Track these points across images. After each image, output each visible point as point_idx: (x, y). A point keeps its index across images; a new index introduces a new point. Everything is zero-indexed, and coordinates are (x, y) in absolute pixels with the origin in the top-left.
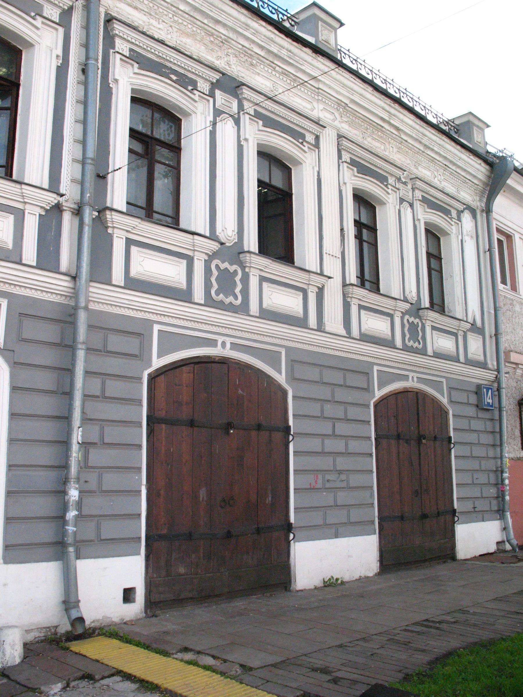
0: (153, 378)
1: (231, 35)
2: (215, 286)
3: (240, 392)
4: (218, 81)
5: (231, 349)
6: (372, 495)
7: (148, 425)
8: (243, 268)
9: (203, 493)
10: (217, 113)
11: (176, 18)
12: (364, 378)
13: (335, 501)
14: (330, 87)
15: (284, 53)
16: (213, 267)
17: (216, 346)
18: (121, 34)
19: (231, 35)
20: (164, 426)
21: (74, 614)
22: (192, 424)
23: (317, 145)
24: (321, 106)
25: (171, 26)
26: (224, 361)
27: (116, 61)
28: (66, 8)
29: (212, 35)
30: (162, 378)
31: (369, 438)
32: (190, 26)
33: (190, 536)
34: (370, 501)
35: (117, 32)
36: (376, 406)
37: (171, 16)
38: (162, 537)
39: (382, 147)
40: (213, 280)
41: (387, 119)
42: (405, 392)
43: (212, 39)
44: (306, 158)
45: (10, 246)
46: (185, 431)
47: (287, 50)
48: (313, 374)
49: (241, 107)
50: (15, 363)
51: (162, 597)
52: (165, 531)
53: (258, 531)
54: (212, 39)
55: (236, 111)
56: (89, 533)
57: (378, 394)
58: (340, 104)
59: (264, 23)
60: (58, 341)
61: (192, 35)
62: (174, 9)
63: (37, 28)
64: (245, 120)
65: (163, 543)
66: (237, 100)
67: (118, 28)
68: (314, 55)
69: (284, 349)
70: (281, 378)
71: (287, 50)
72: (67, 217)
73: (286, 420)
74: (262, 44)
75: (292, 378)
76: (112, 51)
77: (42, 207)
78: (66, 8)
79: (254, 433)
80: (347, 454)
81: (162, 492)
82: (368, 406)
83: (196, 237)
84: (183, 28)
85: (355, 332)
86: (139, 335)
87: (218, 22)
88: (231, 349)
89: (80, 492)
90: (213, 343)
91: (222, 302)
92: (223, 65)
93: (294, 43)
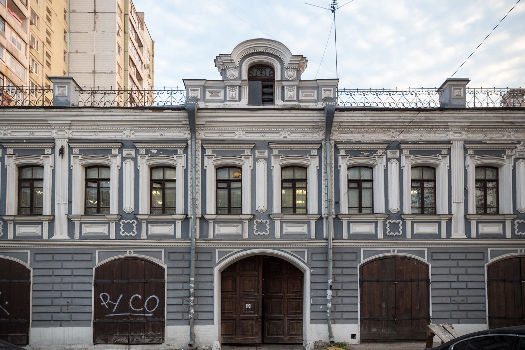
0: (362, 267)
1: (392, 124)
2: (389, 230)
3: (401, 268)
4: (387, 147)
5: (397, 252)
6: (485, 307)
7: (360, 282)
8: (402, 219)
9: (384, 305)
10: (388, 160)
11: (365, 129)
12: (481, 255)
13: (458, 308)
14: (455, 122)
15: (423, 120)
16: (387, 223)
17: (390, 252)
18: (341, 147)
19: (392, 124)
20: (366, 282)
21: (332, 340)
22: (378, 281)
23: (449, 153)
24: (452, 133)
25: (363, 133)
26: (394, 257)
27: (340, 158)
28: (319, 148)
29: (383, 128)
30: (365, 267)
31: (484, 281)
32: (372, 129)
33: (378, 320)
34: (483, 309)
35: (339, 147)
36: (489, 267)
37: (362, 129)
38: (366, 319)
39: (502, 136)
40: (387, 228)
41: (501, 121)
42: (514, 258)
43: (384, 129)
44: (441, 162)
45: (307, 233)
46: (375, 284)
47: (424, 117)
48: (447, 256)
49: (401, 152)
50: (311, 268)
51: (367, 338)
52: (368, 317)
53: (411, 319)
54: (384, 129)
55: (398, 156)
56: (338, 315)
57: (490, 261)
58: (463, 128)
59: (408, 112)
60: (325, 259)
61: (374, 132)
62: (363, 126)
63: (309, 160)
64: (403, 158)
65: (367, 321)
66: (399, 151)
67: (339, 146)
68: (441, 112)
69: (427, 249)
70: (425, 260)
71: (424, 117)
72: (325, 220)
73: (429, 277)
74: (409, 121)
75: (431, 259)
76: (338, 155)
77: (316, 219)
78: (319, 148)
79: (409, 283)
80: (467, 288)
81: (366, 304)
82: (483, 267)
83: (376, 215)
84: (369, 131)
85: (473, 234)
86: (356, 253)
87: (384, 122)
88: (397, 252)
89: (332, 304)
90: (389, 251)
91: (392, 235)
92: (390, 138)
93: (428, 112)
